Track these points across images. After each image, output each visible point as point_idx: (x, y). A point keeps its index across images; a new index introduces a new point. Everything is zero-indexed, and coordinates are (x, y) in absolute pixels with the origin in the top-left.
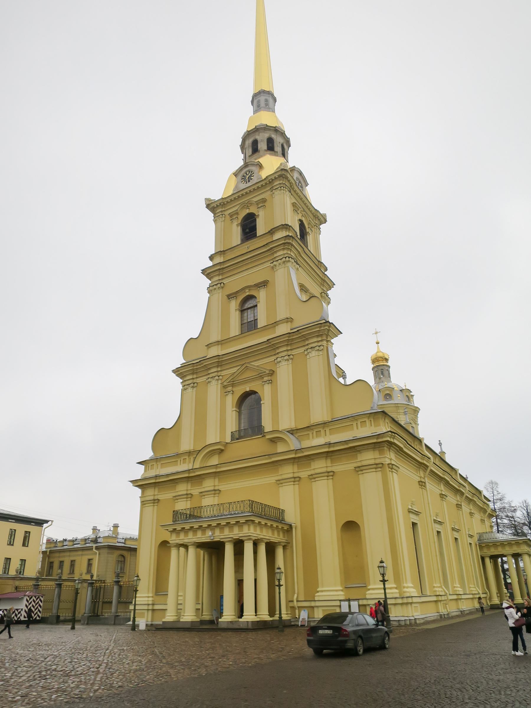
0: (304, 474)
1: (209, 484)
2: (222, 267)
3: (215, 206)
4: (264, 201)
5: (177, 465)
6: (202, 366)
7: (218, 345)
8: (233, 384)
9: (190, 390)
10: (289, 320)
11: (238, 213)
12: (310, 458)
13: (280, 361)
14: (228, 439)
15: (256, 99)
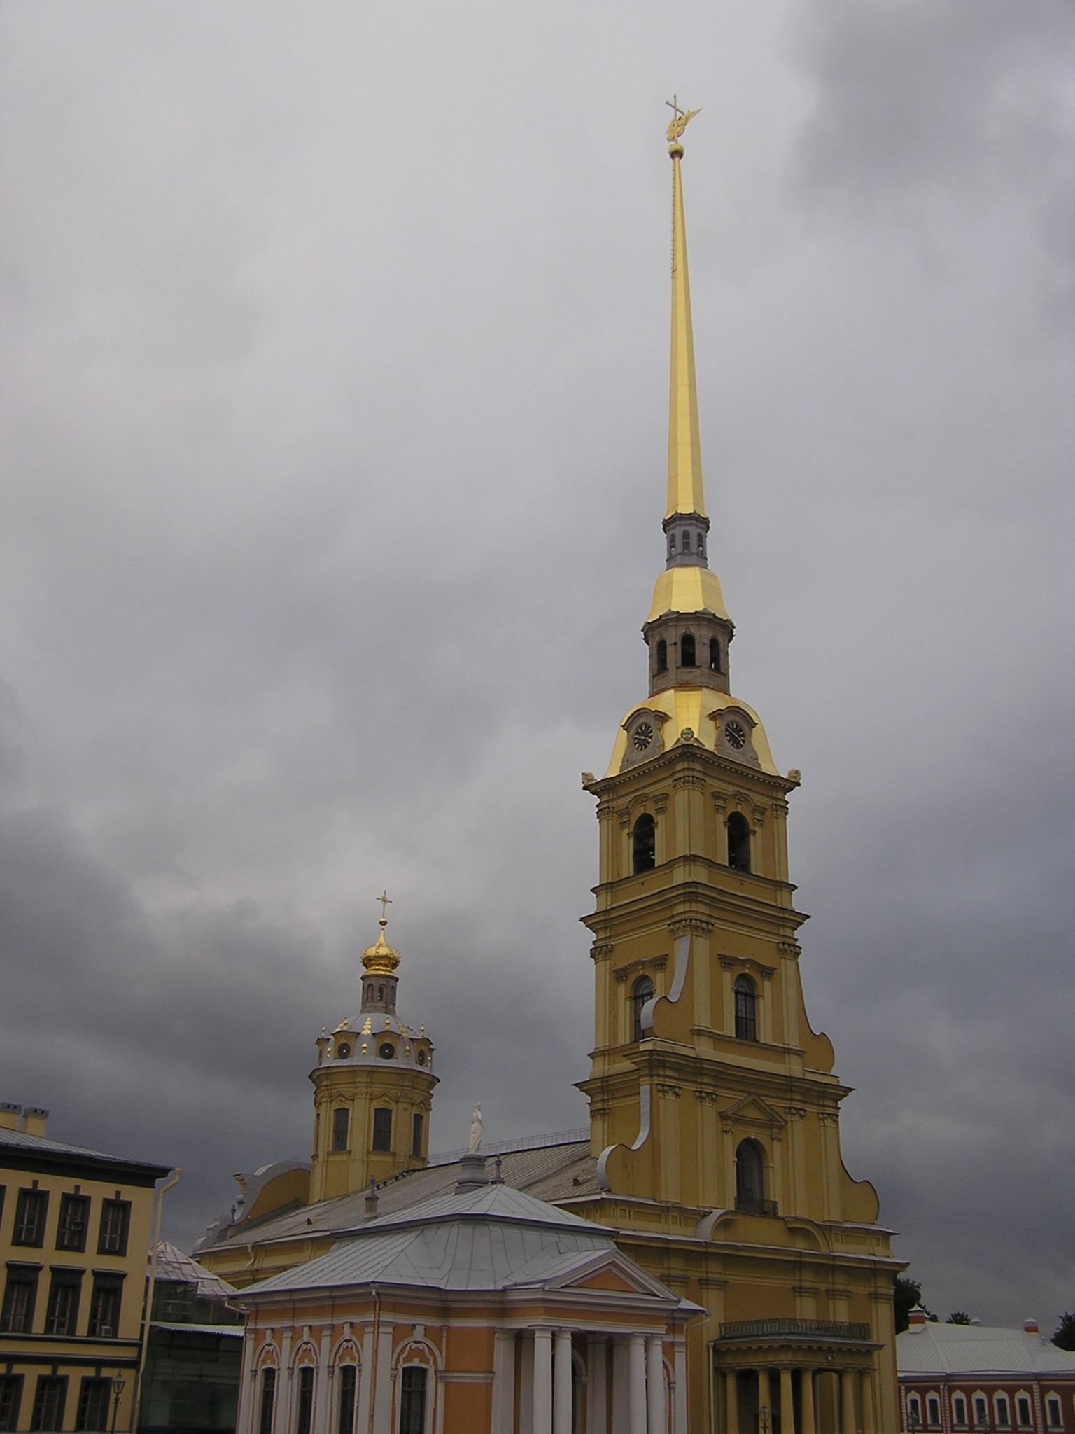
0: (822, 1287)
1: (714, 1270)
2: (719, 897)
3: (699, 755)
4: (762, 811)
5: (660, 1223)
6: (698, 1065)
7: (711, 1037)
8: (736, 1118)
9: (670, 1096)
10: (800, 1054)
11: (727, 799)
12: (833, 1269)
13: (794, 1115)
14: (731, 1205)
15: (696, 526)
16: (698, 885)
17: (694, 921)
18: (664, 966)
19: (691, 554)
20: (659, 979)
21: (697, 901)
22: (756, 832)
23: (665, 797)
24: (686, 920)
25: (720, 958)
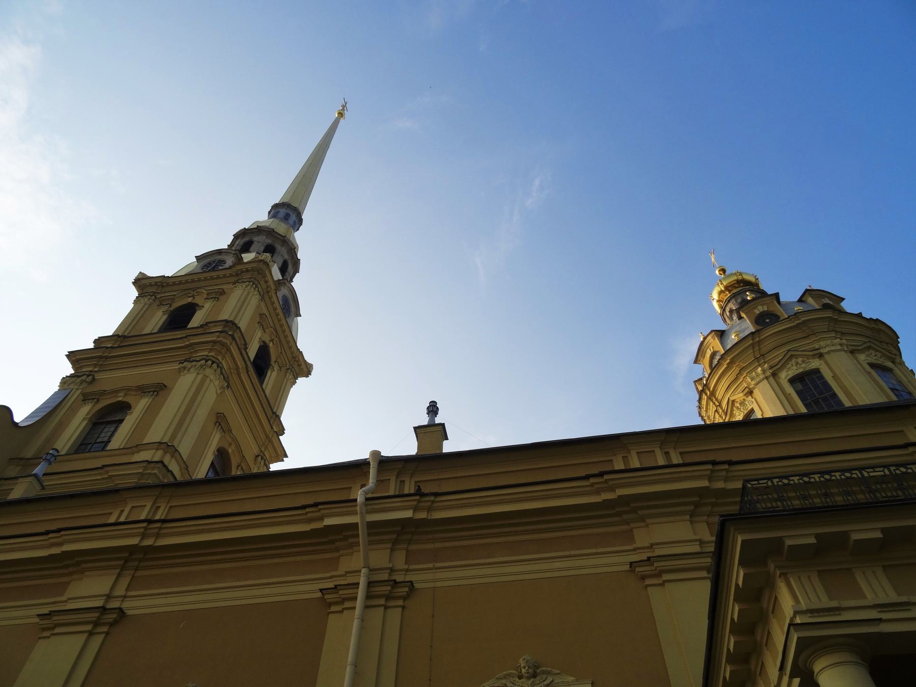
16: (234, 343)
17: (215, 365)
18: (155, 393)
19: (288, 223)
20: (141, 405)
21: (224, 357)
22: (274, 371)
23: (223, 293)
24: (207, 361)
25: (218, 417)
